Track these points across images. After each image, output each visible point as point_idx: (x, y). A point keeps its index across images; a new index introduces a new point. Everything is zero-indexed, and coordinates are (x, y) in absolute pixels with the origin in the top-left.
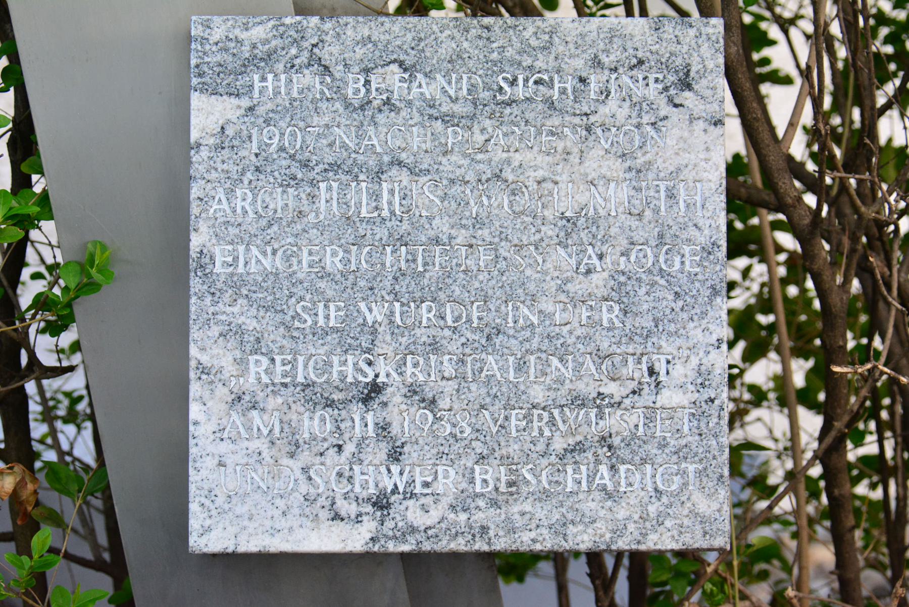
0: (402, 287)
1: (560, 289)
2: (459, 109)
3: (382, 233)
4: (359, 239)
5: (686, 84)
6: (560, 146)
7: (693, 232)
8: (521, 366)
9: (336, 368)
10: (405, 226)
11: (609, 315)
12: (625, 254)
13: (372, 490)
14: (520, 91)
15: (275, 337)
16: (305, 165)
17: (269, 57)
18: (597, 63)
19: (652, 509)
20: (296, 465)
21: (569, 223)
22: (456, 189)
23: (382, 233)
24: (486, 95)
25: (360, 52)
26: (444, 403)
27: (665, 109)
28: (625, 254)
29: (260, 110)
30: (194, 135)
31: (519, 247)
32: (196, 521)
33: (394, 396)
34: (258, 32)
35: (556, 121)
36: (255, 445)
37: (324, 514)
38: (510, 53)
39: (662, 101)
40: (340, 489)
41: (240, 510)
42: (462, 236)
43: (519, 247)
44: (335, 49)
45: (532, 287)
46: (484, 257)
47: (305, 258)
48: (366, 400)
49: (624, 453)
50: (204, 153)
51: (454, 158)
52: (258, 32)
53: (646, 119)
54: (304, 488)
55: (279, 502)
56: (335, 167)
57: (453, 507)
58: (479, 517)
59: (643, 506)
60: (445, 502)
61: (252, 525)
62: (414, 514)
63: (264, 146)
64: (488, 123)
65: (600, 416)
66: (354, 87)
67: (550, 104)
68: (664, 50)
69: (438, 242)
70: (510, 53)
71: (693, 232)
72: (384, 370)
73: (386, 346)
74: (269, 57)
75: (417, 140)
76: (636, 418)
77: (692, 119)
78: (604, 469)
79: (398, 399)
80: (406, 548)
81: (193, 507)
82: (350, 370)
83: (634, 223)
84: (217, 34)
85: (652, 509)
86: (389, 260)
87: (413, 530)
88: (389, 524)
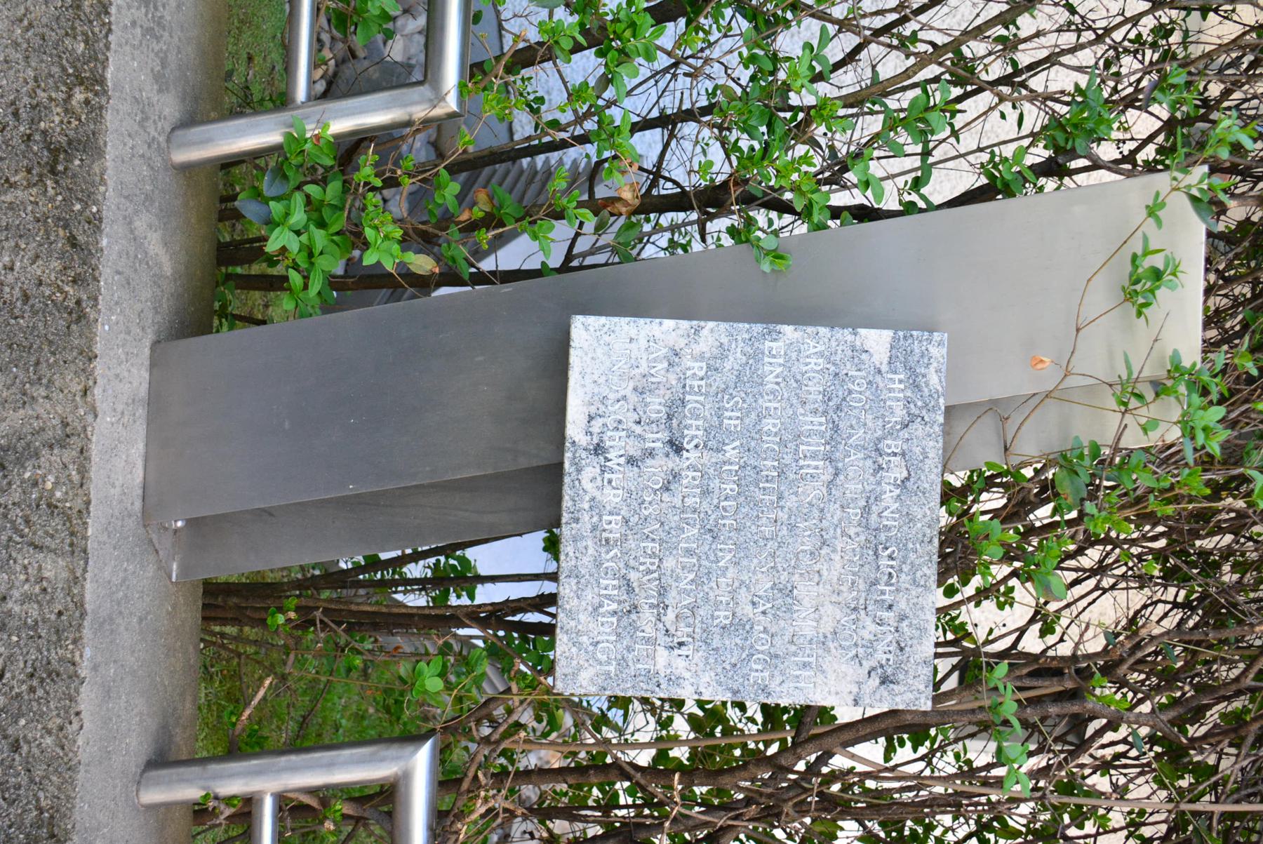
0: (749, 470)
1: (743, 582)
2: (874, 518)
3: (788, 459)
4: (784, 444)
5: (884, 681)
6: (844, 588)
7: (778, 679)
8: (690, 553)
9: (694, 423)
10: (792, 476)
11: (723, 616)
12: (765, 630)
13: (608, 444)
14: (884, 562)
15: (718, 381)
16: (838, 408)
17: (916, 386)
18: (902, 618)
19: (584, 639)
20: (628, 391)
21: (788, 591)
22: (816, 513)
23: (788, 459)
24: (883, 537)
25: (917, 450)
26: (666, 497)
27: (867, 665)
28: (765, 630)
29: (878, 379)
30: (862, 331)
31: (773, 555)
32: (592, 320)
33: (673, 462)
34: (934, 379)
35: (862, 586)
36: (644, 364)
37: (593, 410)
38: (912, 556)
39: (874, 663)
40: (610, 421)
41: (599, 351)
42: (783, 516)
43: (773, 555)
44: (920, 433)
45: (745, 563)
46: (768, 530)
47: (772, 405)
48: (671, 443)
49: (625, 621)
50: (850, 338)
51: (838, 512)
52: (934, 379)
53: (861, 651)
54: (612, 396)
55: (604, 378)
56: (836, 428)
57: (593, 499)
58: (585, 517)
59: (587, 633)
60: (597, 494)
61: (588, 359)
62: (590, 472)
63: (853, 380)
64: (863, 538)
65: (652, 606)
66: (891, 445)
67: (875, 583)
68: (910, 666)
69: (780, 498)
70: (912, 556)
71: (778, 679)
72: (692, 456)
73: (708, 458)
74: (916, 386)
75: (853, 487)
76: (649, 631)
77: (859, 683)
78: (614, 606)
79: (671, 465)
80: (567, 465)
81: (603, 319)
82: (693, 432)
83: (786, 638)
84: (934, 351)
85: (584, 639)
86: (769, 463)
87: (579, 471)
88: (584, 455)
